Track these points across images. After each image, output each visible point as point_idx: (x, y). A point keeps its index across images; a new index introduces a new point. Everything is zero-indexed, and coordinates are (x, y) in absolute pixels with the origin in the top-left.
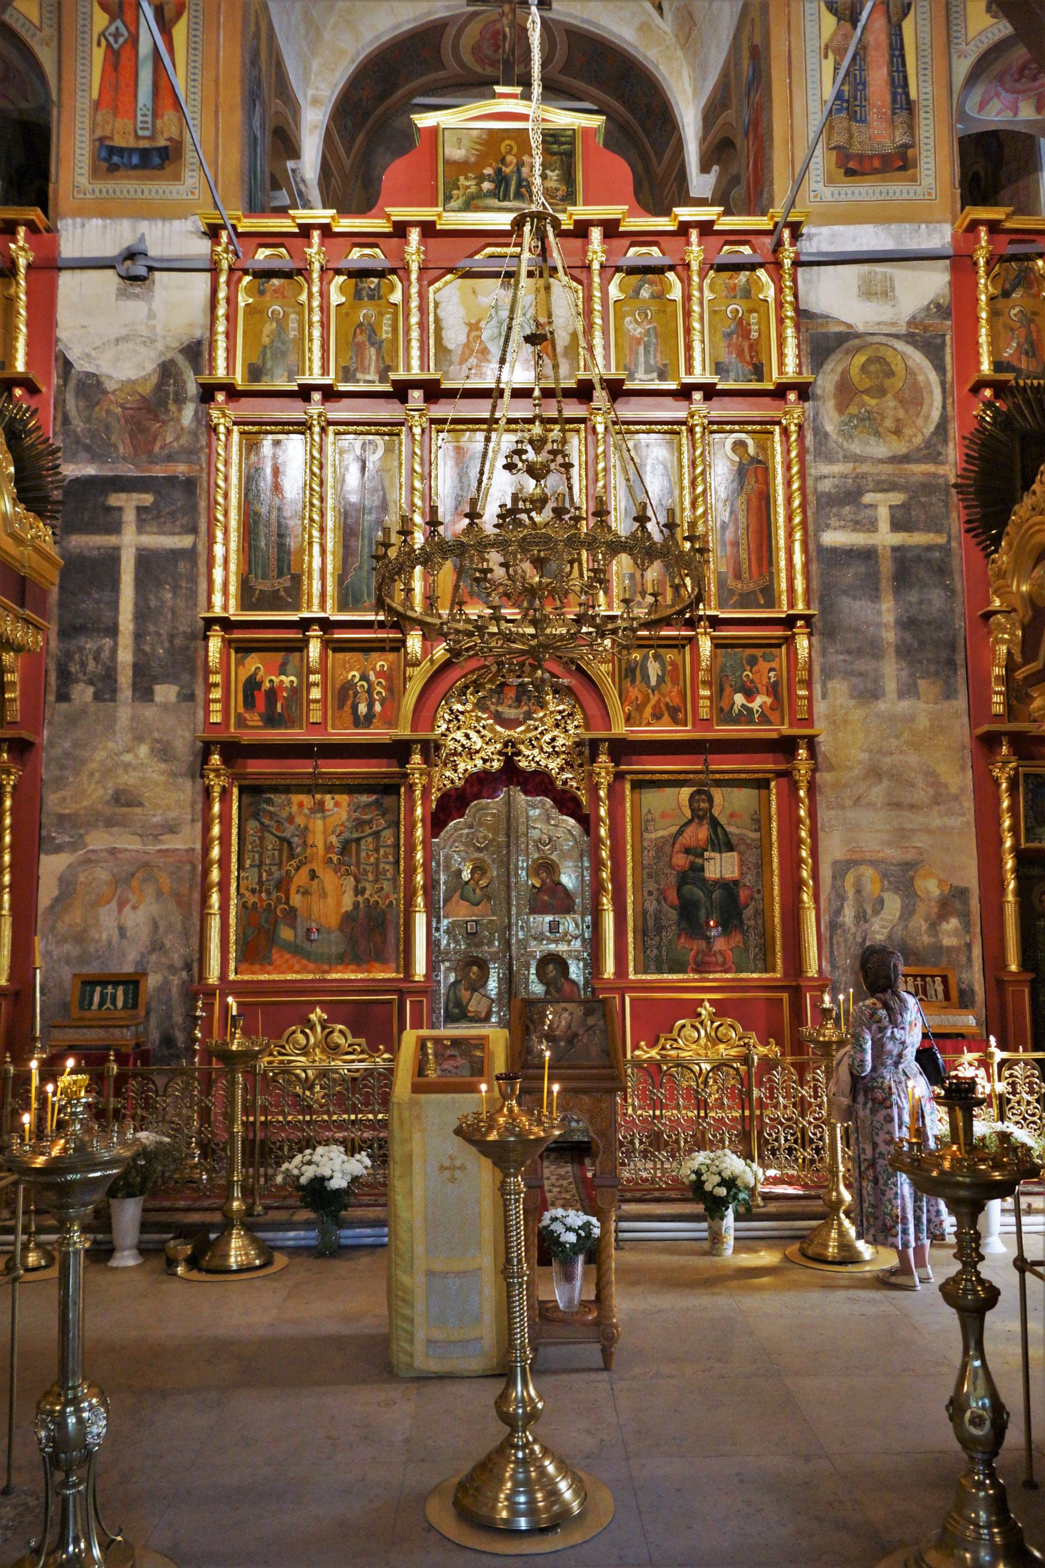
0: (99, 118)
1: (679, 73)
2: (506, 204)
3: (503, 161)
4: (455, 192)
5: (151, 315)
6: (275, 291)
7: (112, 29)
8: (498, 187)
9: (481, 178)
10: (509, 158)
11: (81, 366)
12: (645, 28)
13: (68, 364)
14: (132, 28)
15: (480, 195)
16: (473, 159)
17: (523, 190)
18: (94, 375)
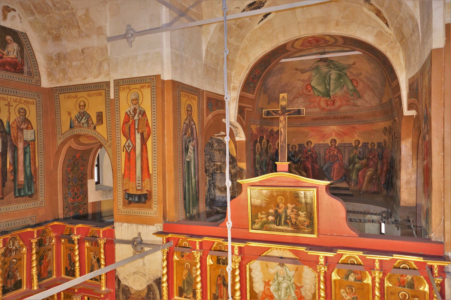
0: (125, 181)
1: (398, 55)
2: (280, 227)
3: (278, 206)
4: (257, 220)
5: (144, 265)
6: (187, 256)
7: (127, 144)
8: (276, 218)
9: (268, 214)
10: (281, 205)
11: (123, 282)
12: (380, 35)
13: (119, 281)
14: (133, 143)
15: (267, 222)
16: (264, 205)
17: (288, 221)
18: (127, 286)
